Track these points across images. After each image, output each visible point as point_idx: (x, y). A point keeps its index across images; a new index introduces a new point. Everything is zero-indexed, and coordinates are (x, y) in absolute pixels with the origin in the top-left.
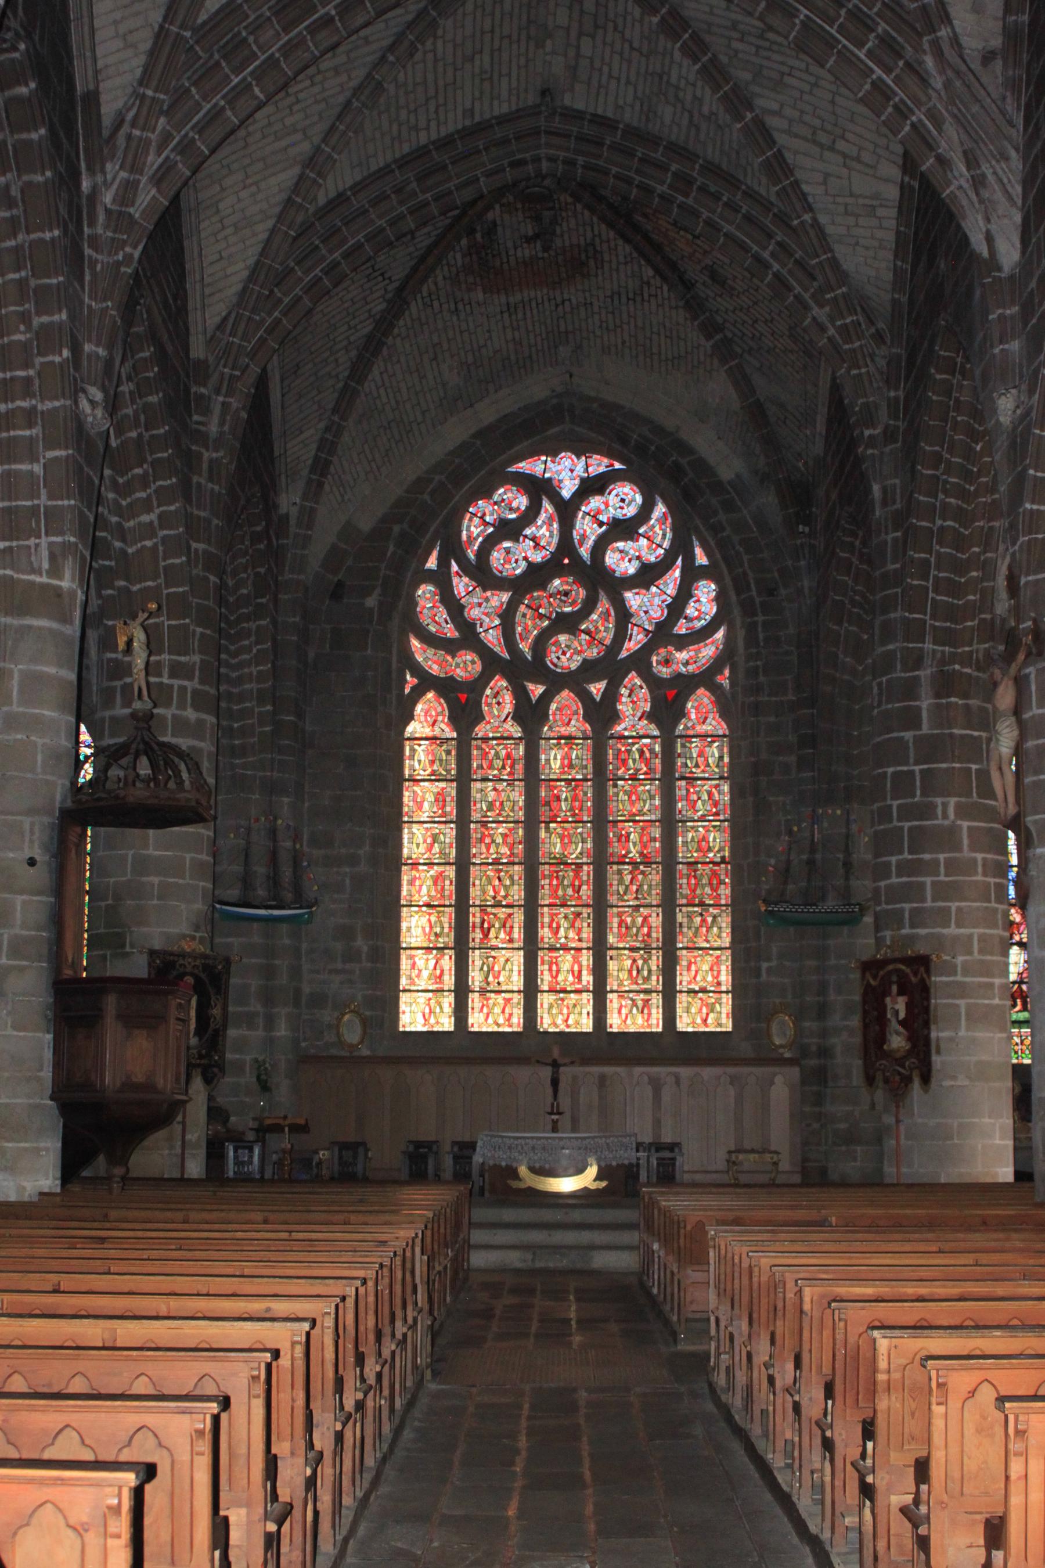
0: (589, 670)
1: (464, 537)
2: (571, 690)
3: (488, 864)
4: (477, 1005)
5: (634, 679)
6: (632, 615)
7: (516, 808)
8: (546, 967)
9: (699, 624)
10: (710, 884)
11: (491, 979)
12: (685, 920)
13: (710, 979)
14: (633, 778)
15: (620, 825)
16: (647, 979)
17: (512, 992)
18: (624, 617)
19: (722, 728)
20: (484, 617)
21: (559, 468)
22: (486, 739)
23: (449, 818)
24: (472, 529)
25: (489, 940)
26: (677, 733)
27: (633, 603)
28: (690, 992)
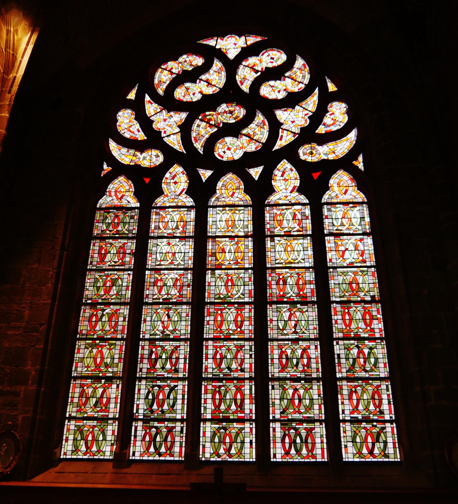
0: (249, 159)
1: (156, 81)
2: (234, 173)
3: (159, 304)
4: (140, 433)
5: (285, 165)
6: (282, 124)
7: (186, 258)
8: (210, 396)
9: (334, 128)
10: (364, 319)
11: (155, 407)
12: (342, 352)
13: (372, 407)
14: (288, 235)
15: (278, 271)
16: (309, 408)
17: (175, 420)
18: (275, 127)
19: (360, 197)
20: (167, 128)
21: (227, 42)
22: (163, 208)
23: (127, 267)
24: (163, 77)
25: (155, 370)
26: (323, 201)
27: (282, 116)
28: (354, 421)
